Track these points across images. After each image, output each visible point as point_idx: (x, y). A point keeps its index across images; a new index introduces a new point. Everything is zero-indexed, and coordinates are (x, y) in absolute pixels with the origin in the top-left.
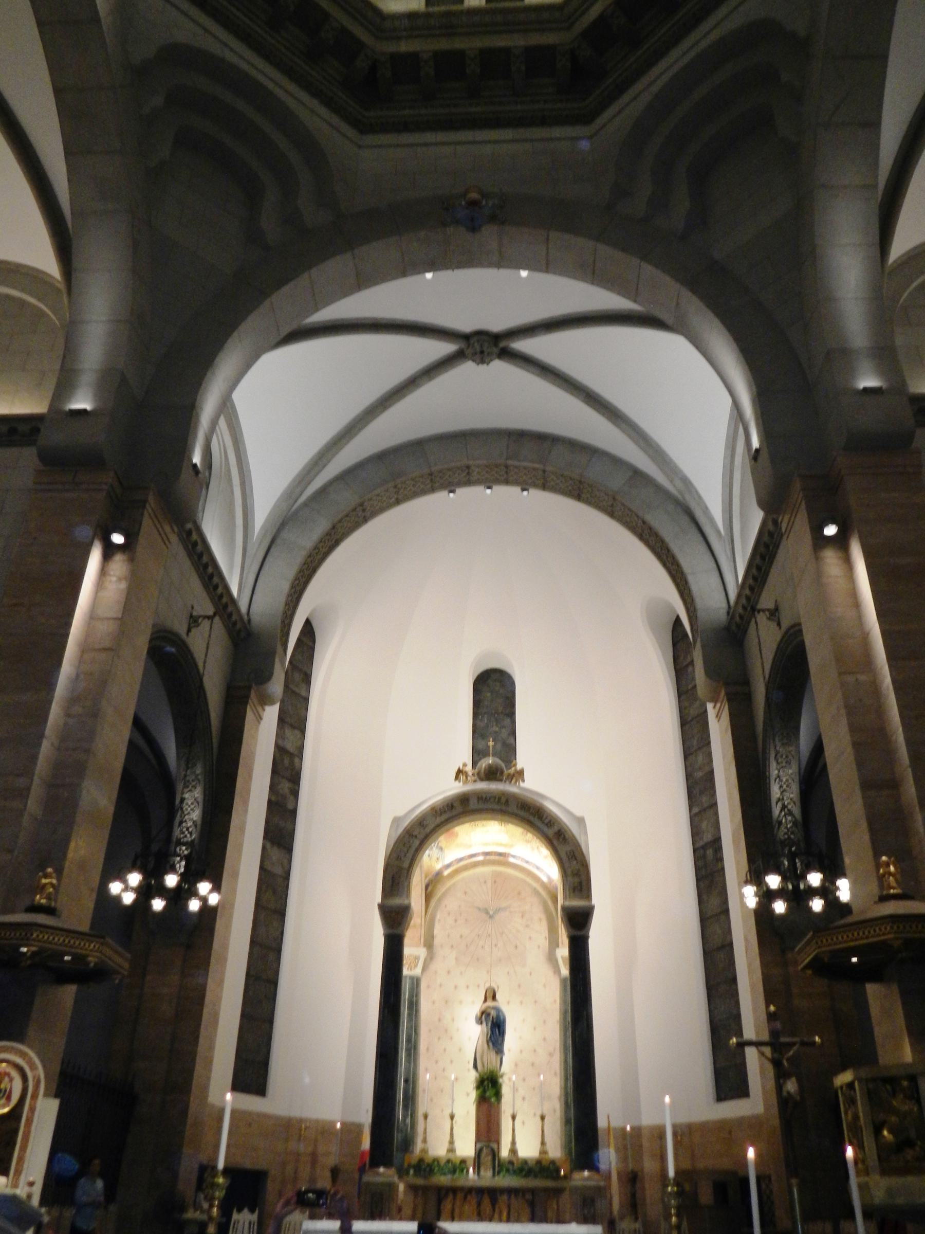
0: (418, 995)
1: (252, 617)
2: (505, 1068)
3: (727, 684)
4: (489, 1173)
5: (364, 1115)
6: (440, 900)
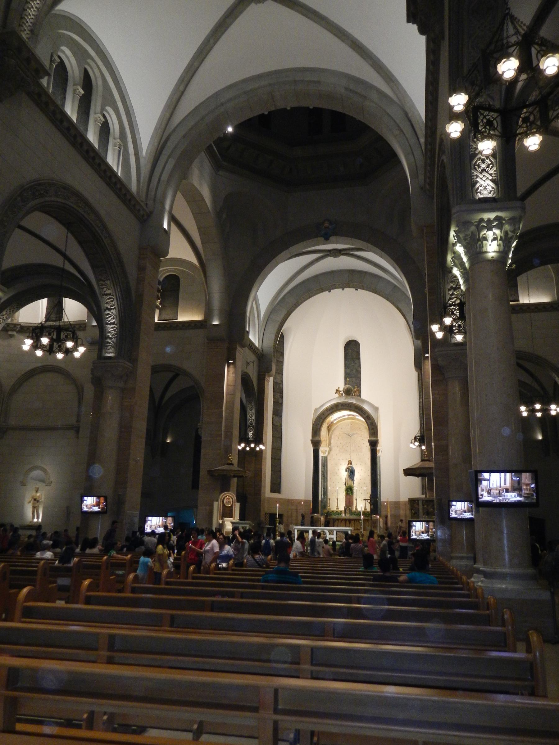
0: (327, 462)
1: (264, 349)
4: (349, 515)
5: (311, 498)
6: (333, 431)
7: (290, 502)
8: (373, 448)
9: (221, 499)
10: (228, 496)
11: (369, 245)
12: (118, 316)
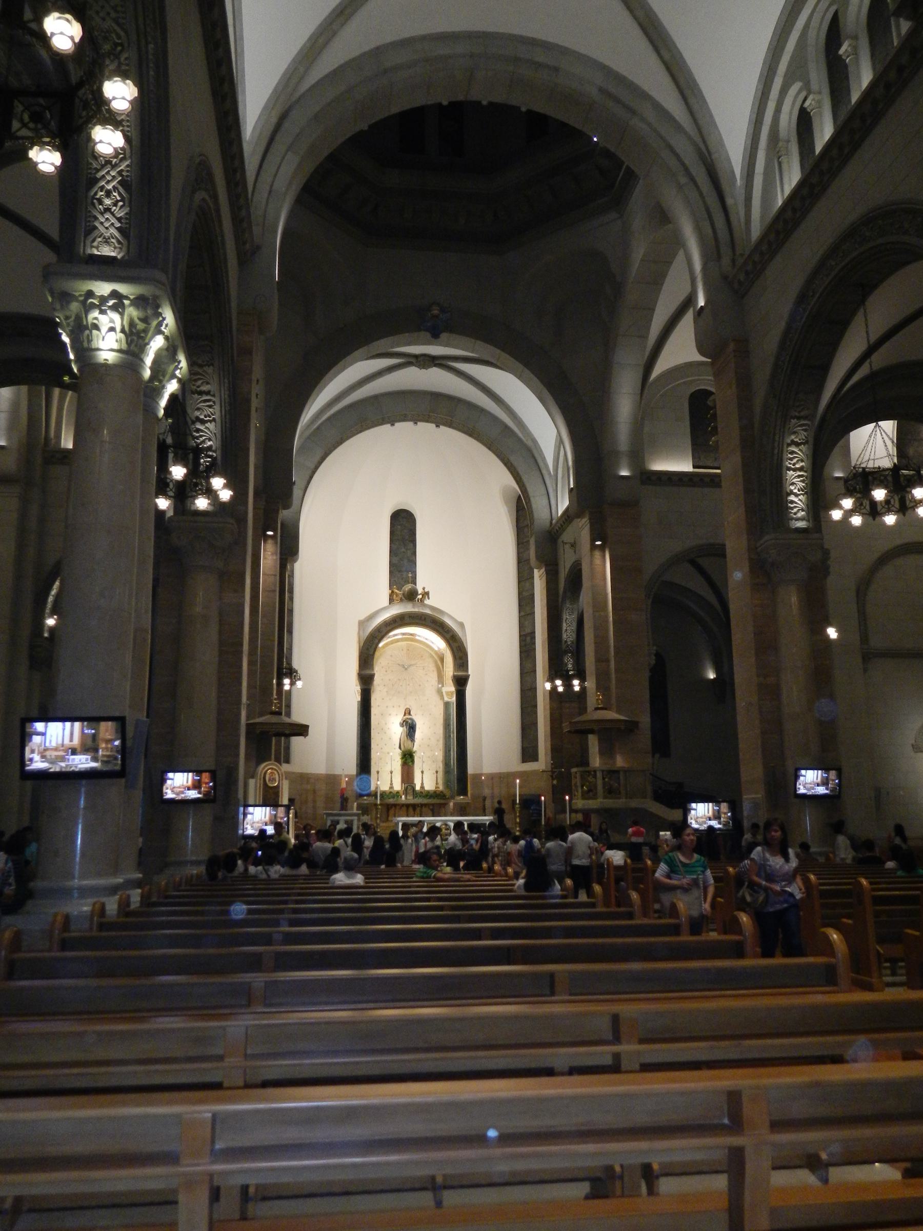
2: (415, 749)
3: (546, 565)
4: (411, 798)
7: (303, 778)
8: (460, 688)
9: (261, 776)
10: (272, 769)
11: (504, 355)
12: (219, 436)
